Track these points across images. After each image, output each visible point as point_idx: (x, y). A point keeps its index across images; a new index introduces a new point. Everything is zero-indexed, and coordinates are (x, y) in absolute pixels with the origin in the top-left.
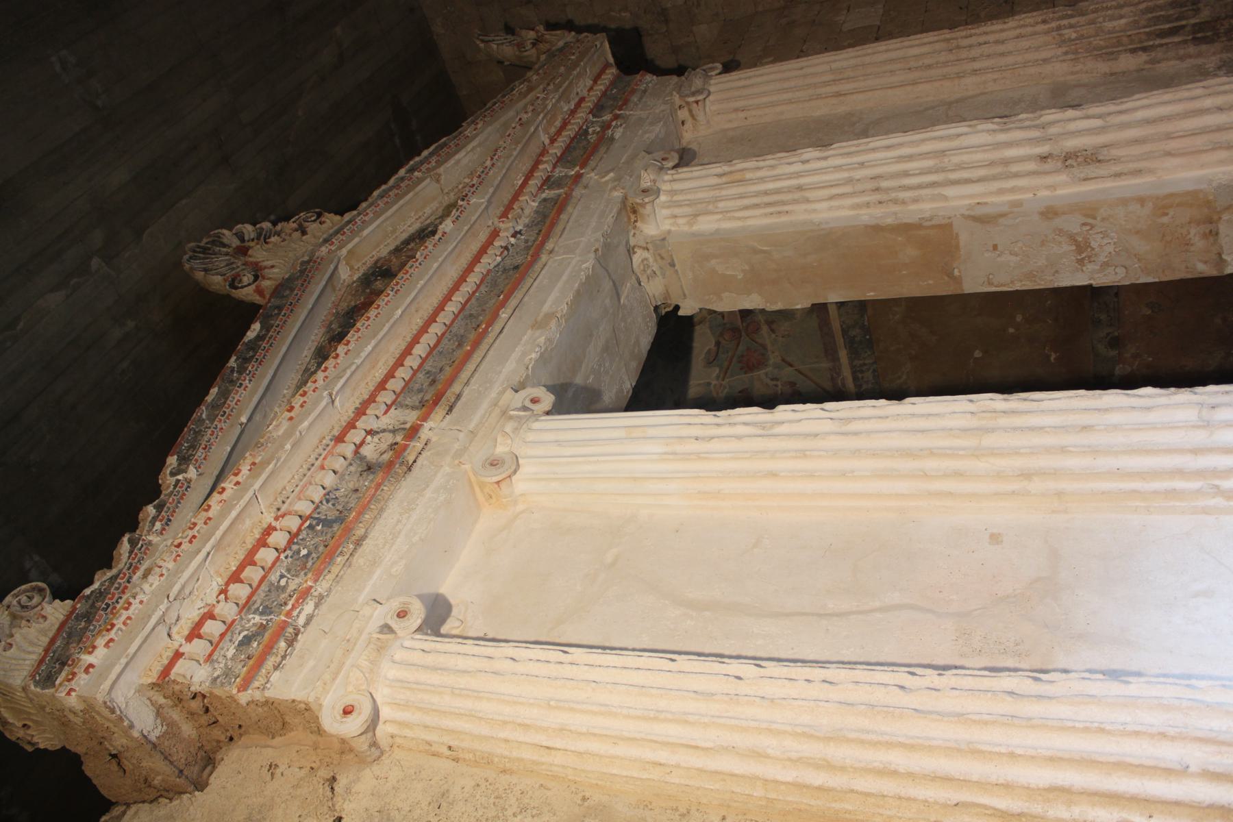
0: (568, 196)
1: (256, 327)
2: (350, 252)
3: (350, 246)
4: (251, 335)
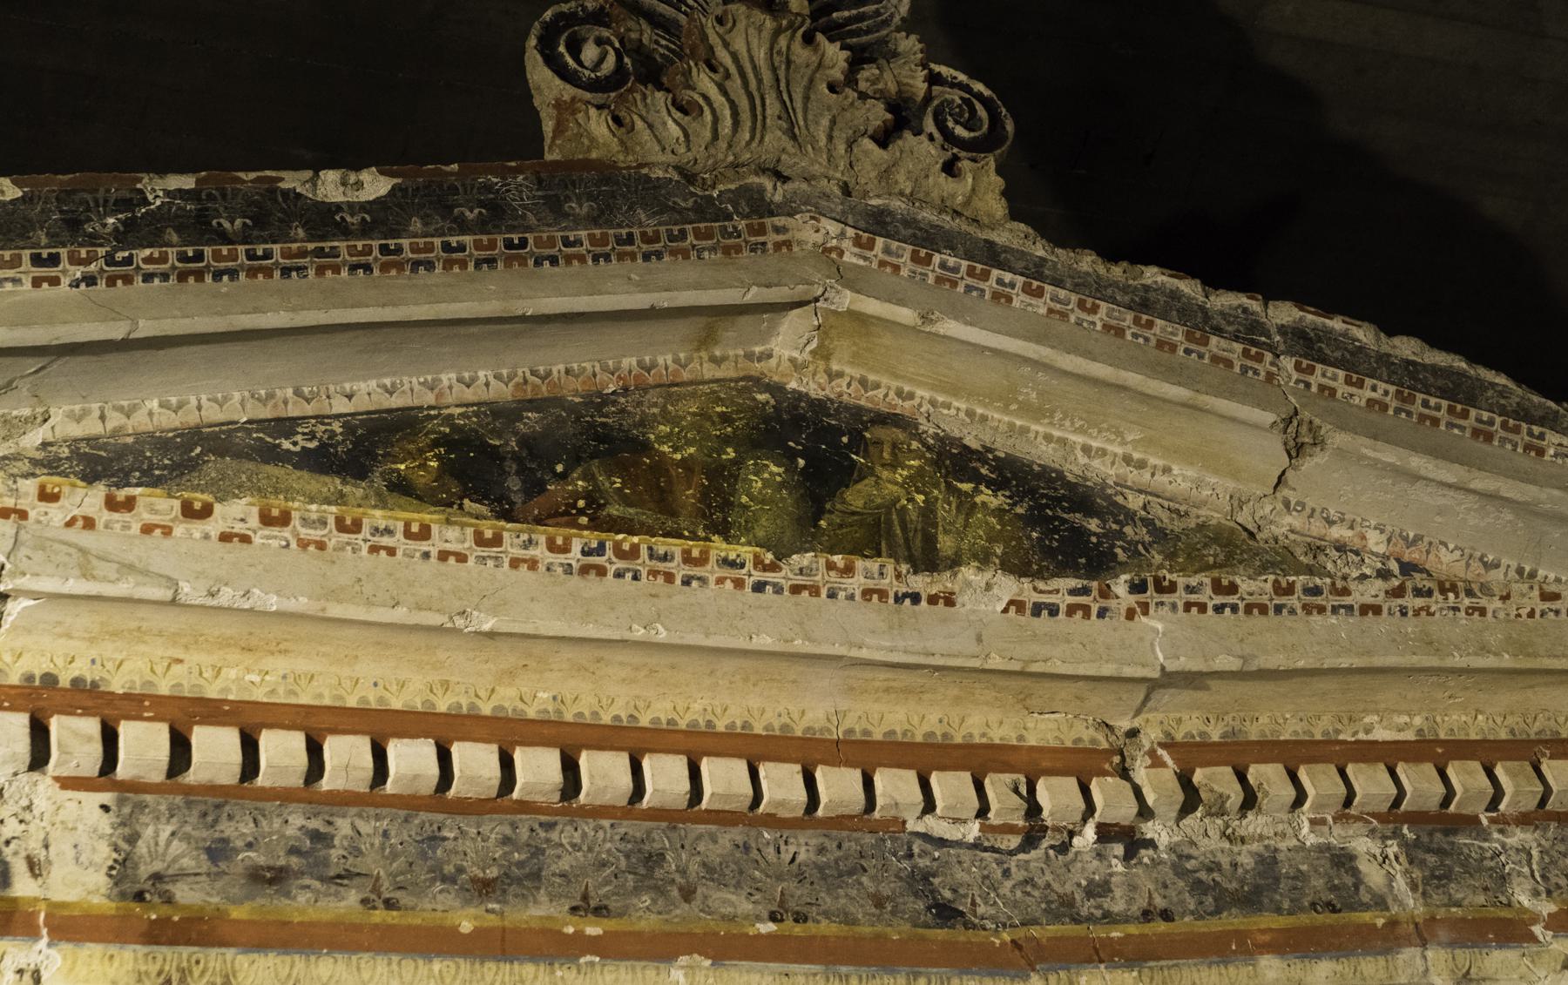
0: (1388, 939)
1: (375, 185)
2: (855, 316)
3: (872, 306)
4: (330, 186)
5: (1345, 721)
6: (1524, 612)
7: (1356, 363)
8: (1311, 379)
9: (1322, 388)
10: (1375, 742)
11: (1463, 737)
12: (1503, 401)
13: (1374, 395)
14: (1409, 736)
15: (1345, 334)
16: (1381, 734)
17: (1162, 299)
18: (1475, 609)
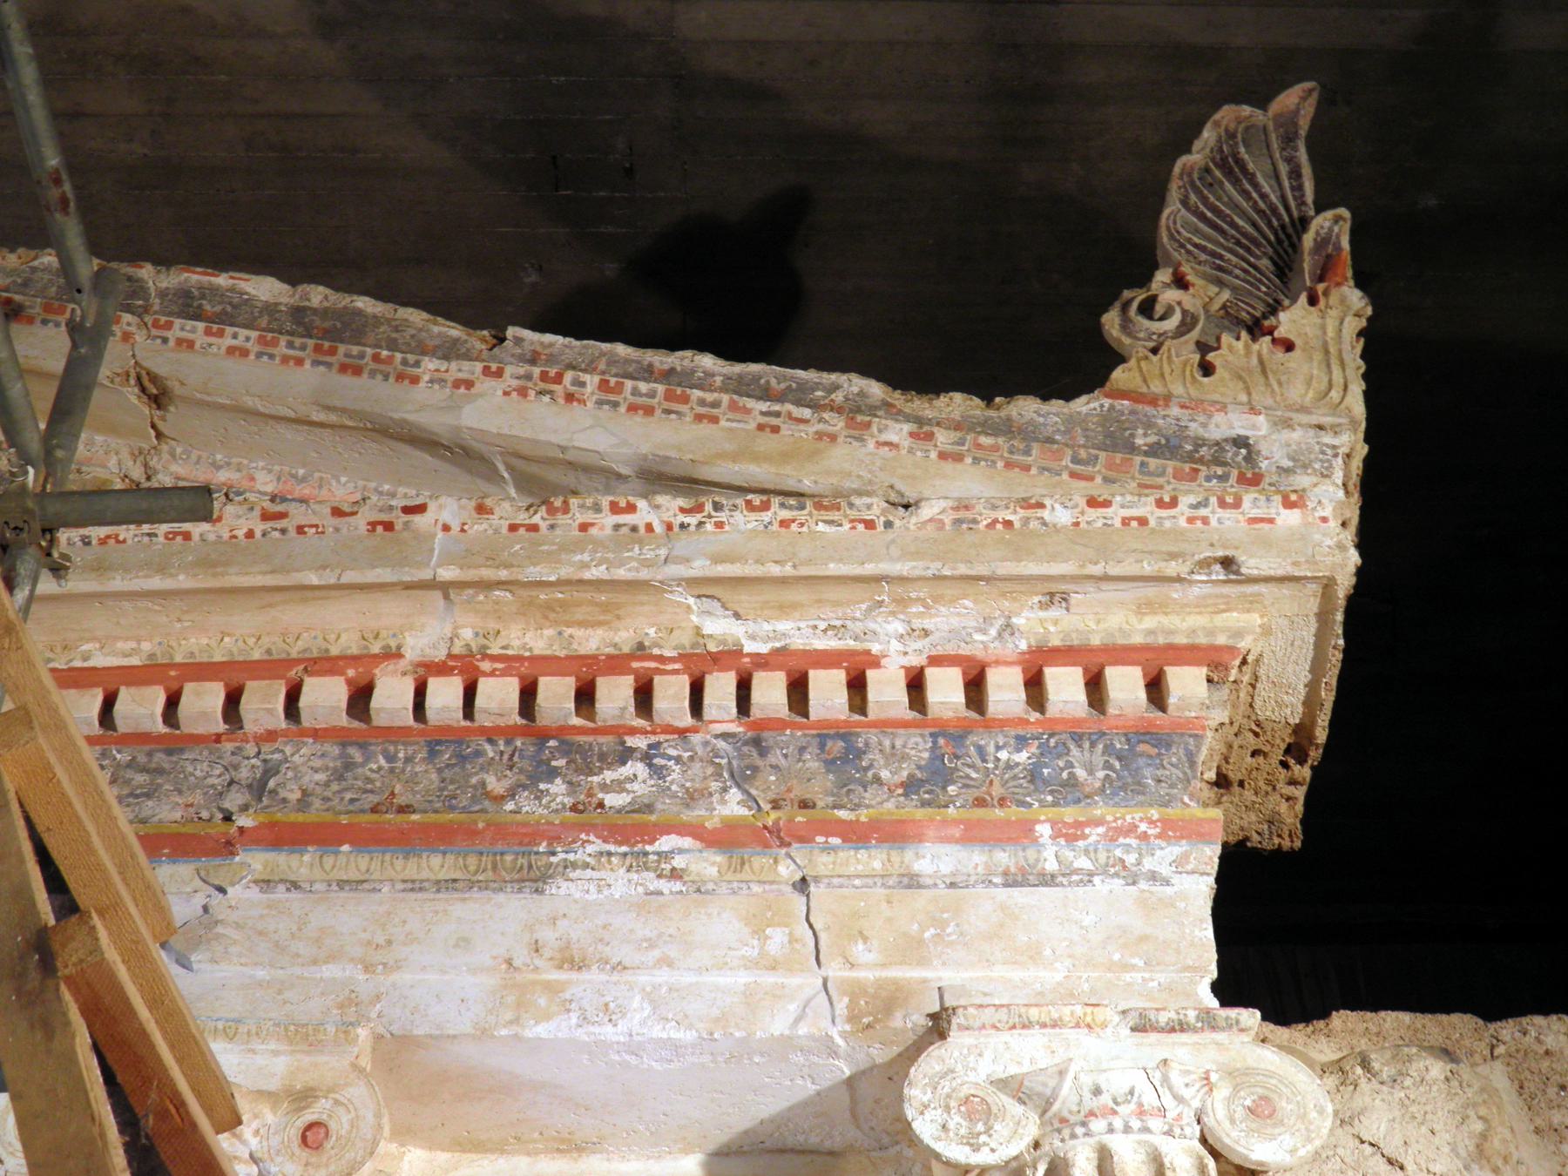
5: (59, 650)
6: (240, 533)
7: (231, 314)
8: (169, 334)
9: (179, 342)
10: (94, 669)
11: (205, 660)
12: (394, 335)
13: (234, 342)
14: (135, 661)
15: (232, 289)
16: (100, 661)
17: (46, 277)
18: (176, 534)
